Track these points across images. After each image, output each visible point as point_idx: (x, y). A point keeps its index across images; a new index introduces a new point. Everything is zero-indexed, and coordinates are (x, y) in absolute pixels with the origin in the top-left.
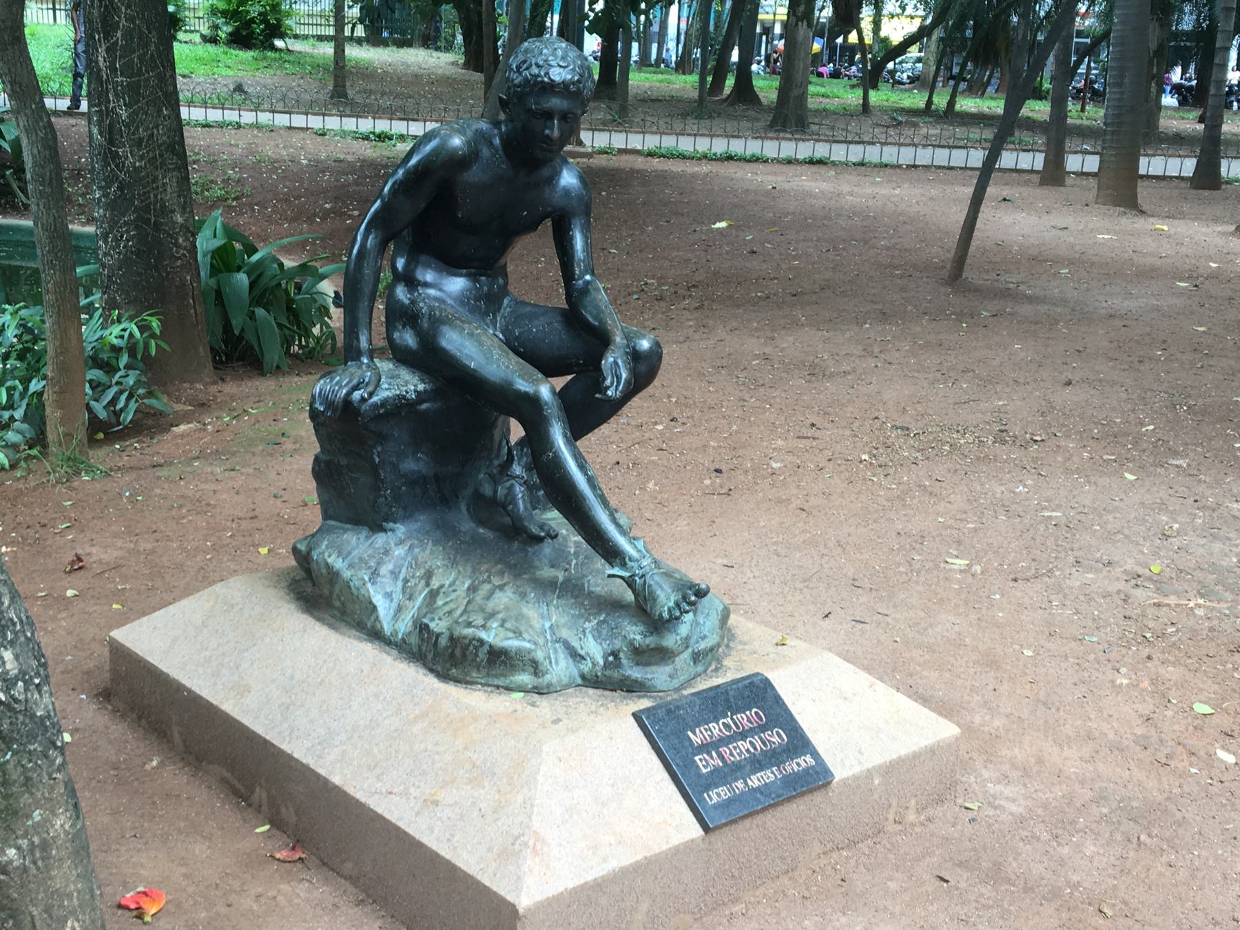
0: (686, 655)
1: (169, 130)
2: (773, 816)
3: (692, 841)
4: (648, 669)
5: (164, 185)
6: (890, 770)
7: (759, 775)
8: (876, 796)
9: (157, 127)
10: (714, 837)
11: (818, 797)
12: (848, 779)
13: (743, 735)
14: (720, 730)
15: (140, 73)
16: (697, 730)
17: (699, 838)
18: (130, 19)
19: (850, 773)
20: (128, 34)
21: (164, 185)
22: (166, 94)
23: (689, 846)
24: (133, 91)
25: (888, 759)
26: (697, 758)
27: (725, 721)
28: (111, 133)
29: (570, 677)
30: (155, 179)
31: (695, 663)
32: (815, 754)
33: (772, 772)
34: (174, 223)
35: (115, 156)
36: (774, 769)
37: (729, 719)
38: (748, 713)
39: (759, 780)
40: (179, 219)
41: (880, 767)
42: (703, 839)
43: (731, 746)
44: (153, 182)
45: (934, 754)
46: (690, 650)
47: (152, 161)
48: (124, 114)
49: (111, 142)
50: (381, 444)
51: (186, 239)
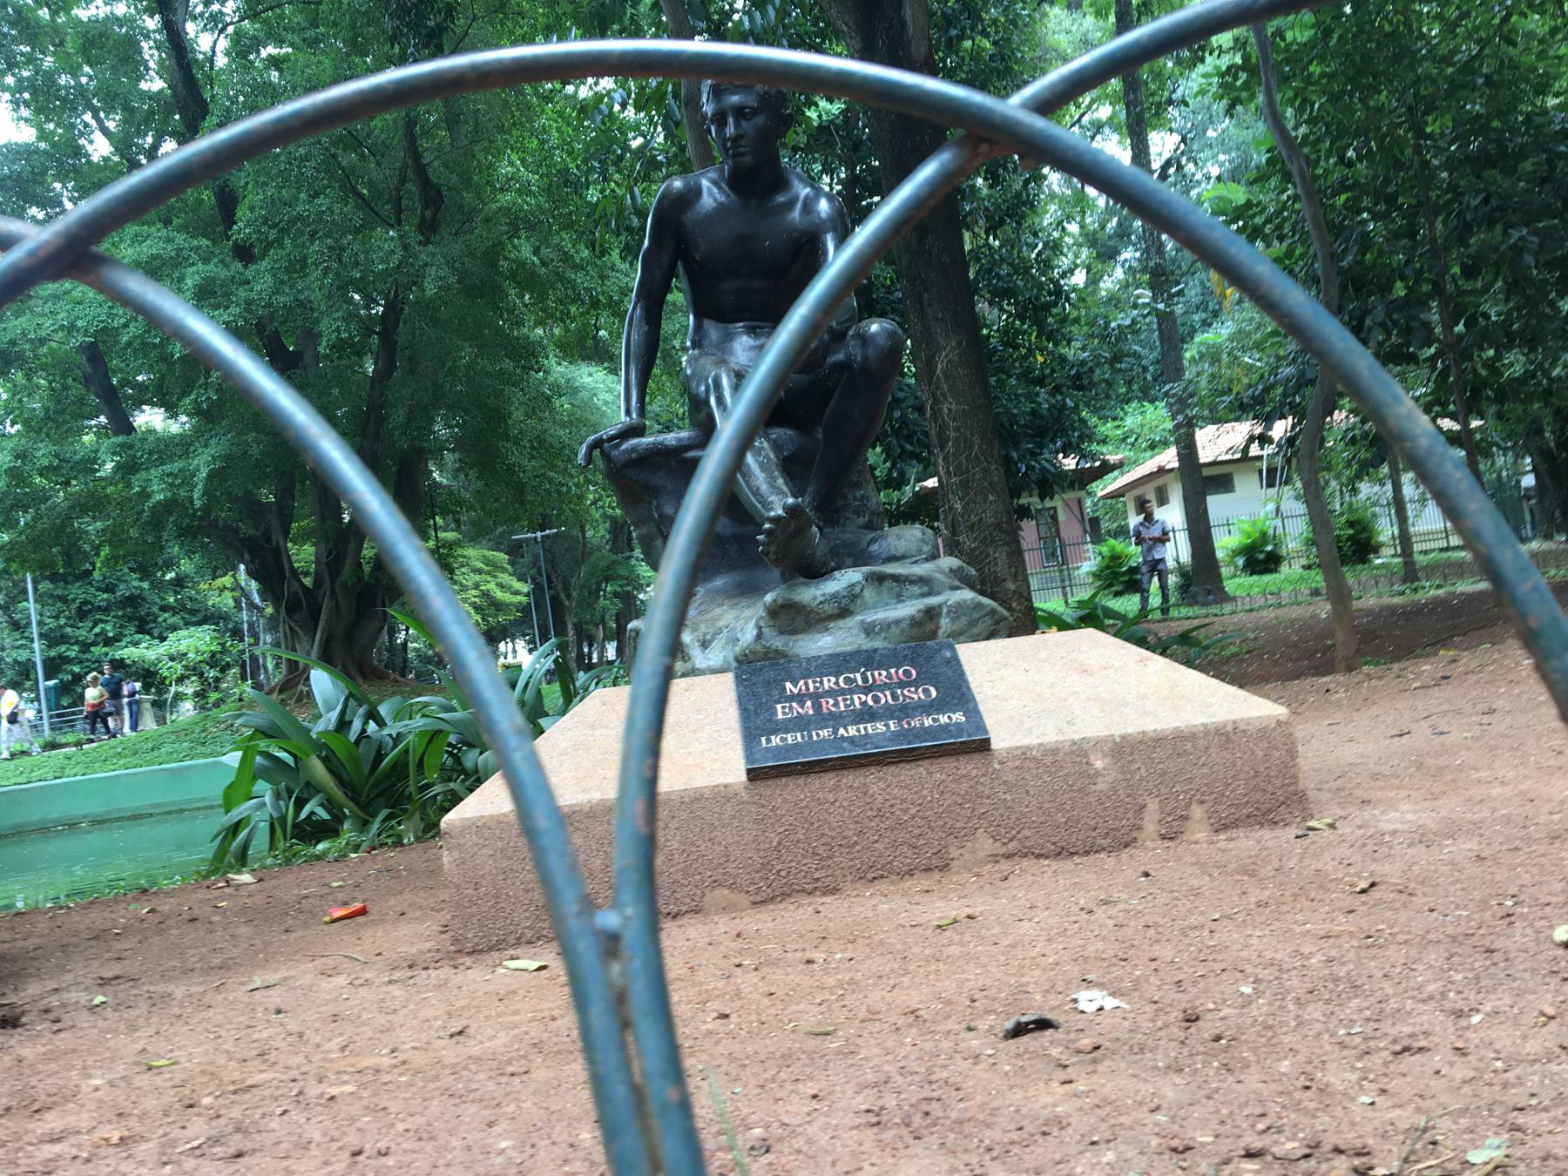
0: (852, 622)
1: (996, 512)
2: (881, 779)
3: (726, 786)
4: (793, 638)
5: (995, 559)
6: (1125, 749)
7: (861, 726)
8: (1101, 786)
9: (985, 511)
10: (767, 788)
11: (968, 766)
12: (1030, 748)
13: (866, 690)
14: (837, 683)
15: (967, 471)
16: (802, 682)
17: (735, 784)
18: (957, 429)
19: (1035, 742)
20: (957, 443)
21: (995, 559)
22: (991, 484)
23: (722, 795)
24: (964, 485)
25: (1118, 731)
26: (779, 707)
27: (852, 676)
28: (953, 526)
29: (725, 662)
30: (988, 556)
31: (868, 635)
32: (972, 711)
33: (887, 726)
34: (1007, 590)
35: (958, 543)
36: (891, 723)
37: (858, 676)
38: (893, 671)
39: (858, 730)
40: (1011, 586)
41: (1098, 742)
42: (746, 788)
43: (840, 698)
44: (986, 557)
45: (1228, 740)
46: (859, 618)
47: (983, 540)
48: (958, 506)
49: (954, 533)
50: (656, 498)
51: (1019, 604)
